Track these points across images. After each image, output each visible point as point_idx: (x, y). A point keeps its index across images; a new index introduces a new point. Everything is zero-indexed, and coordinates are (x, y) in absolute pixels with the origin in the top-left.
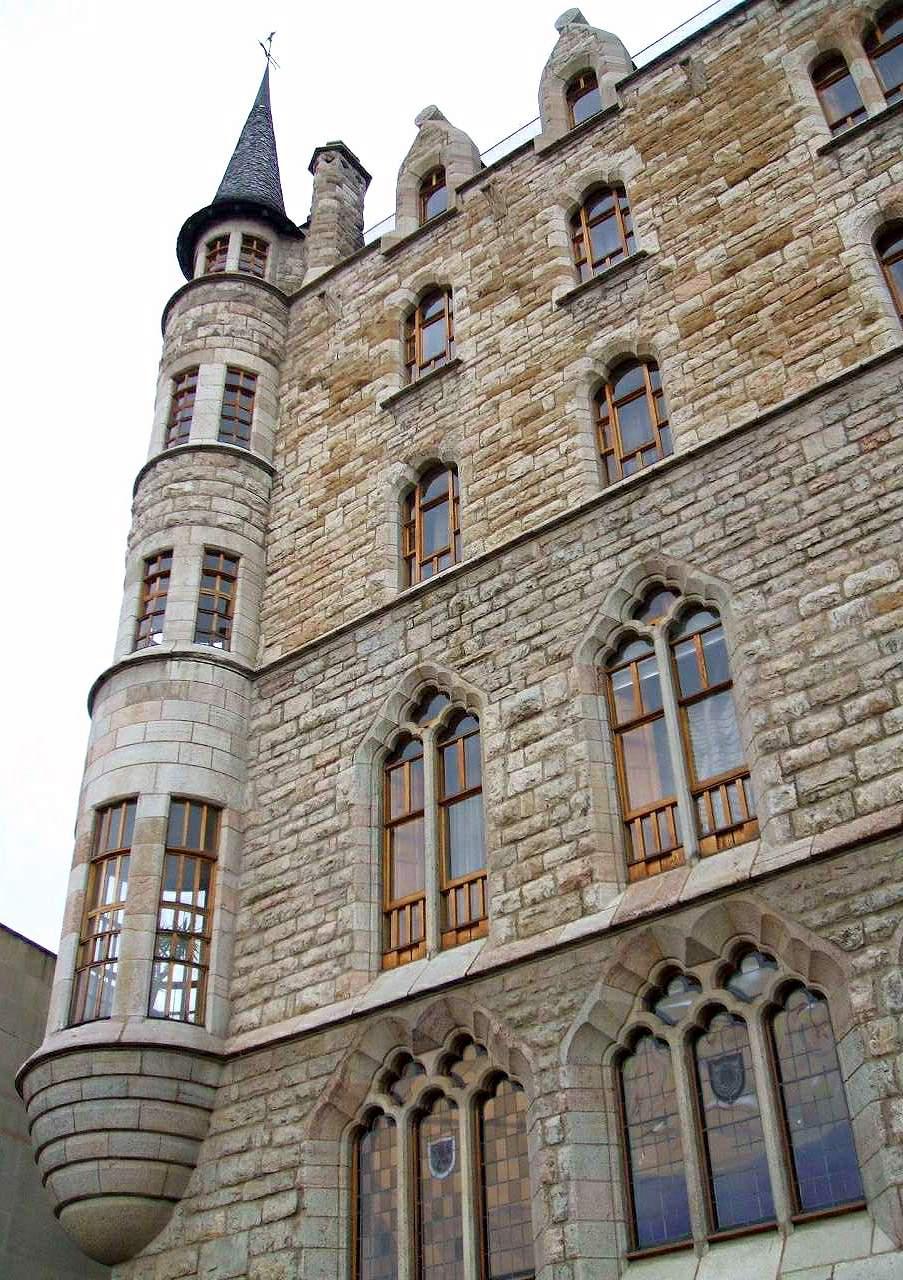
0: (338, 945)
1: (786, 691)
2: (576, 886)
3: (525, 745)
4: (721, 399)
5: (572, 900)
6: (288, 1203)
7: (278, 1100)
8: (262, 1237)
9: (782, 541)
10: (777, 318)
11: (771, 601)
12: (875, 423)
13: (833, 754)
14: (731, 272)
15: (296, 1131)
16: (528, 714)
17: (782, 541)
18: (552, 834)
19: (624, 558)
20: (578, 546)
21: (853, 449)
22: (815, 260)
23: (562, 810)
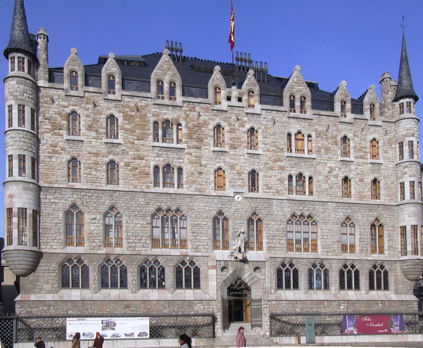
0: (61, 241)
1: (130, 232)
2: (100, 246)
3: (93, 223)
4: (129, 182)
5: (99, 248)
6: (55, 274)
7: (52, 260)
8: (50, 278)
9: (133, 211)
10: (139, 173)
11: (130, 219)
12: (148, 201)
13: (134, 242)
14: (134, 159)
15: (56, 266)
16: (95, 219)
17: (133, 211)
18: (96, 238)
19: (111, 202)
20: (104, 195)
21: (144, 203)
22: (146, 166)
23: (98, 235)
